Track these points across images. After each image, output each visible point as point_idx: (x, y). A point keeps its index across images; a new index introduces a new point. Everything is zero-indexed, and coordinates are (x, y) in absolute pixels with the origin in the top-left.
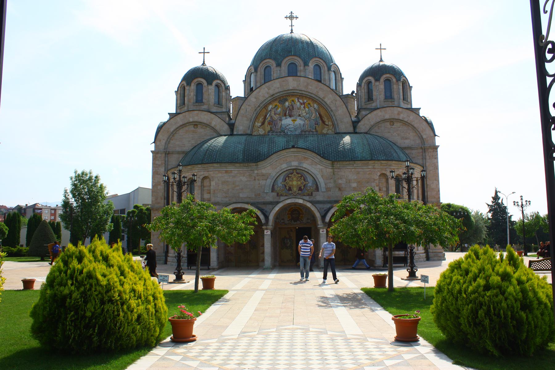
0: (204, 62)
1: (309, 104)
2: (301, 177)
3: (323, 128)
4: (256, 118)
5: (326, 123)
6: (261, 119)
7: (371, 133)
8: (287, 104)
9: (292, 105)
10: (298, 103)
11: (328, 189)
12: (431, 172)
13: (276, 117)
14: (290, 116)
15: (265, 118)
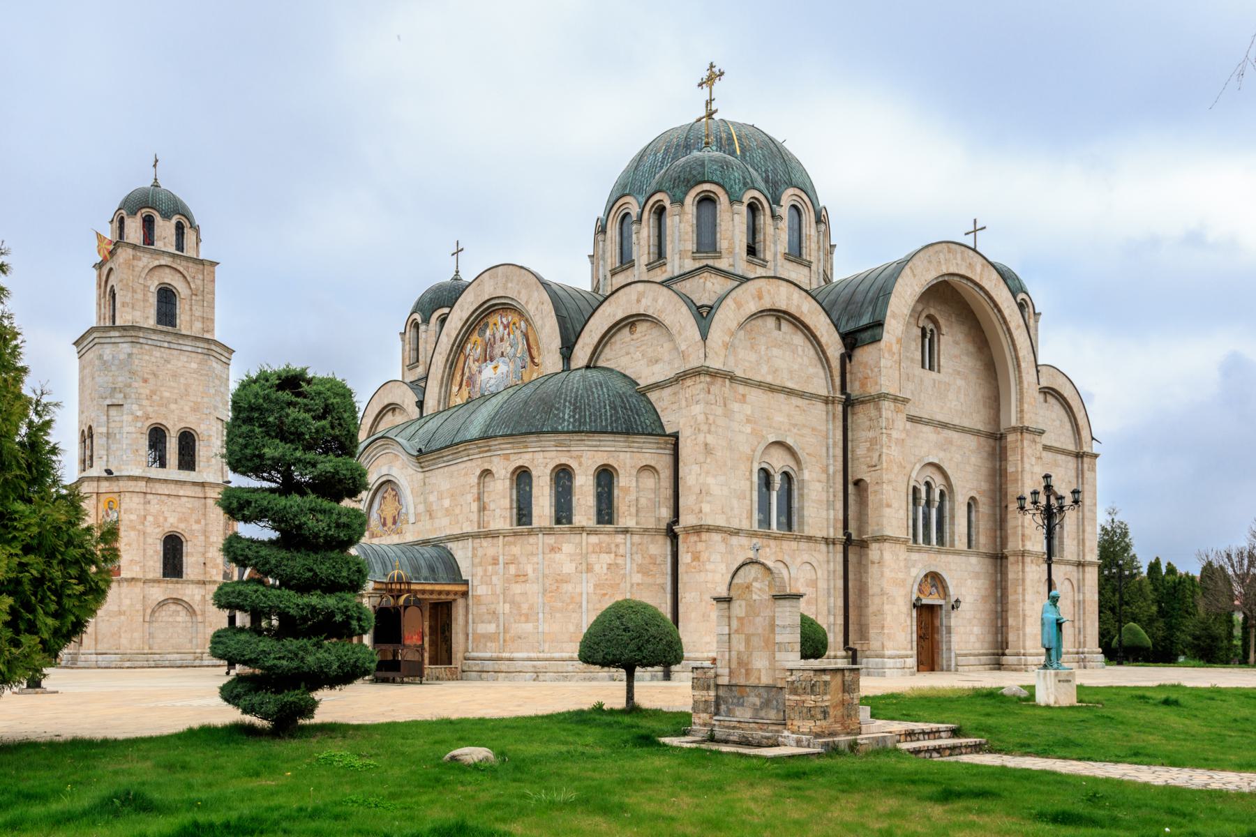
0: (457, 272)
1: (514, 324)
2: (395, 496)
3: (532, 372)
4: (451, 376)
5: (536, 361)
6: (458, 378)
7: (600, 363)
8: (488, 333)
9: (494, 335)
10: (501, 328)
11: (417, 515)
12: (689, 441)
13: (475, 367)
14: (491, 361)
15: (463, 374)
